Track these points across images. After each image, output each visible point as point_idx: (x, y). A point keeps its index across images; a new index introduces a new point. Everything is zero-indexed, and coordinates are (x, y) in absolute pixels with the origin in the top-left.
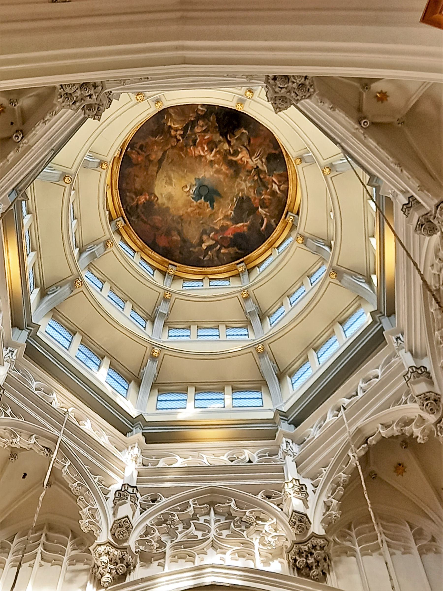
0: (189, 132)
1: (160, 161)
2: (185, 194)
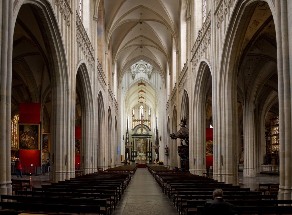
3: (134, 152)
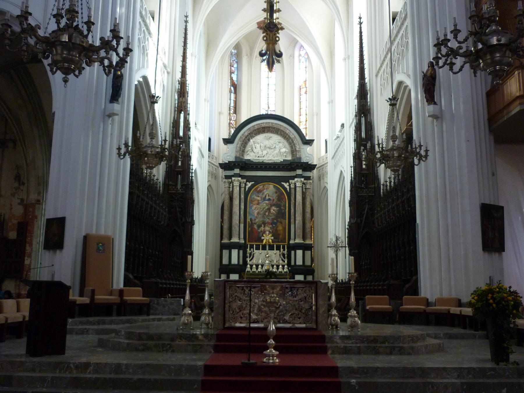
3: (230, 247)
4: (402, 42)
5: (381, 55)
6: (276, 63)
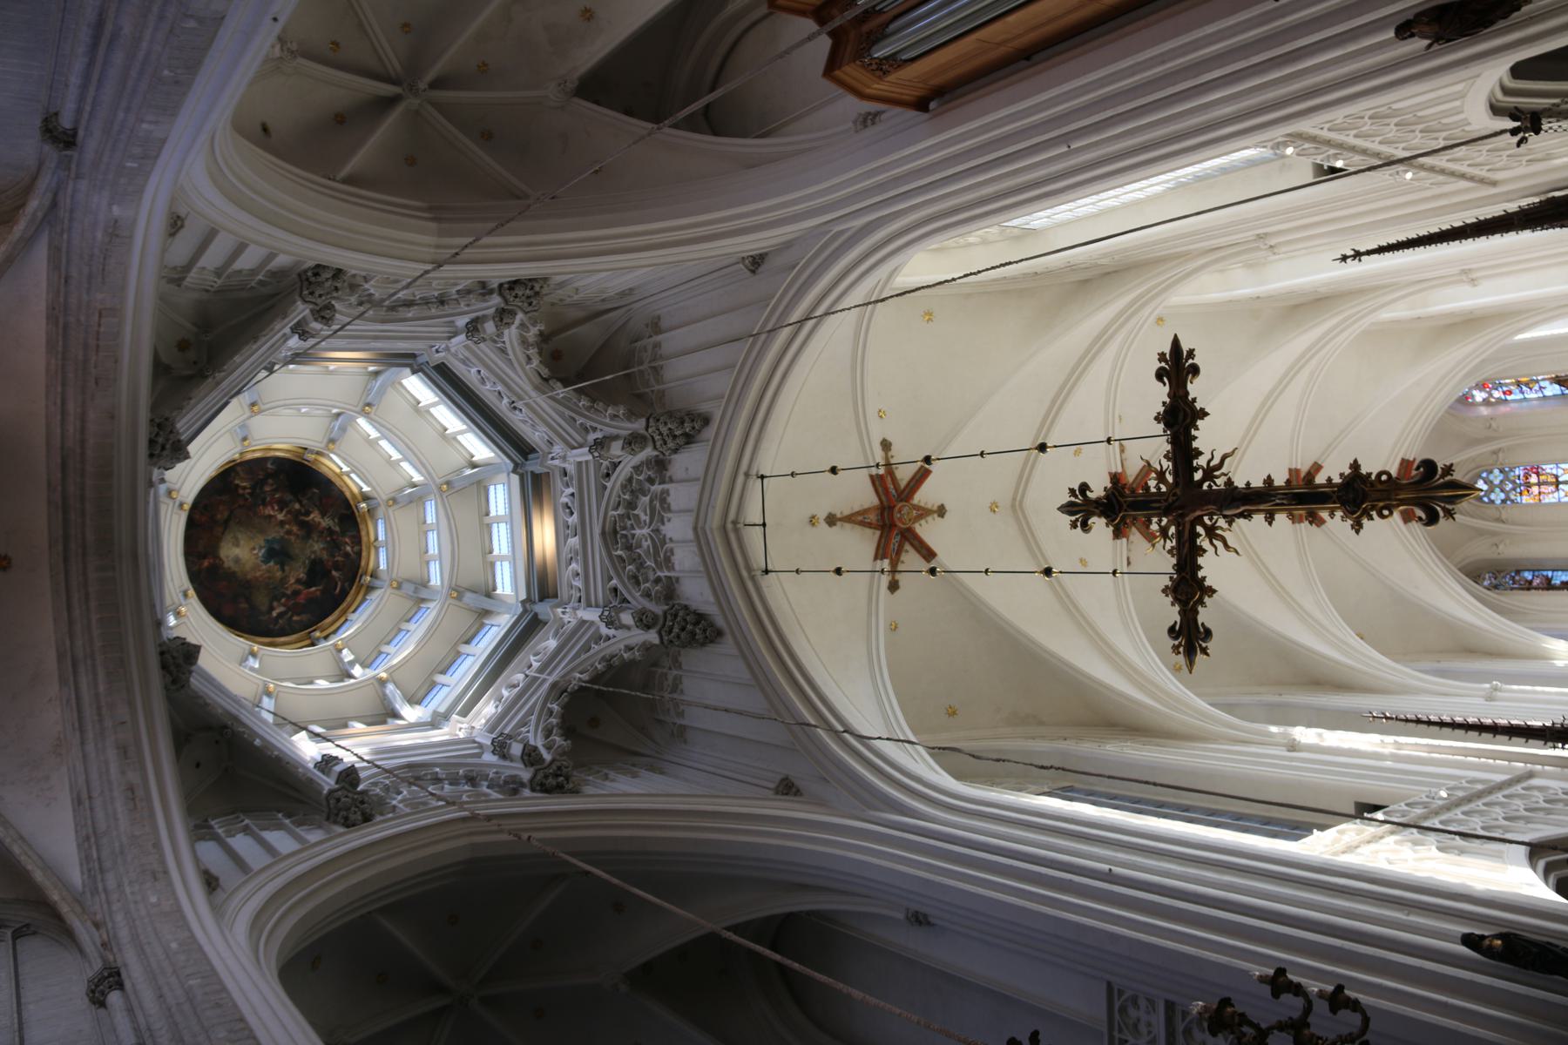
0: (258, 491)
1: (226, 523)
2: (253, 557)
4: (1400, 140)
5: (1432, 184)
6: (1454, 477)
